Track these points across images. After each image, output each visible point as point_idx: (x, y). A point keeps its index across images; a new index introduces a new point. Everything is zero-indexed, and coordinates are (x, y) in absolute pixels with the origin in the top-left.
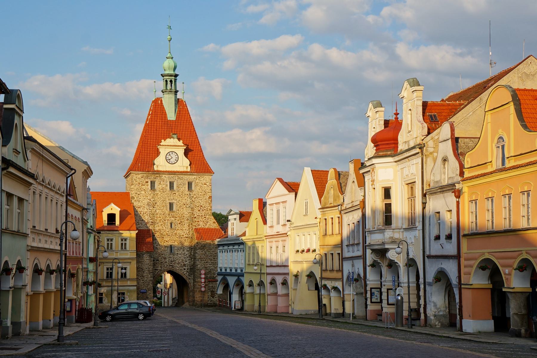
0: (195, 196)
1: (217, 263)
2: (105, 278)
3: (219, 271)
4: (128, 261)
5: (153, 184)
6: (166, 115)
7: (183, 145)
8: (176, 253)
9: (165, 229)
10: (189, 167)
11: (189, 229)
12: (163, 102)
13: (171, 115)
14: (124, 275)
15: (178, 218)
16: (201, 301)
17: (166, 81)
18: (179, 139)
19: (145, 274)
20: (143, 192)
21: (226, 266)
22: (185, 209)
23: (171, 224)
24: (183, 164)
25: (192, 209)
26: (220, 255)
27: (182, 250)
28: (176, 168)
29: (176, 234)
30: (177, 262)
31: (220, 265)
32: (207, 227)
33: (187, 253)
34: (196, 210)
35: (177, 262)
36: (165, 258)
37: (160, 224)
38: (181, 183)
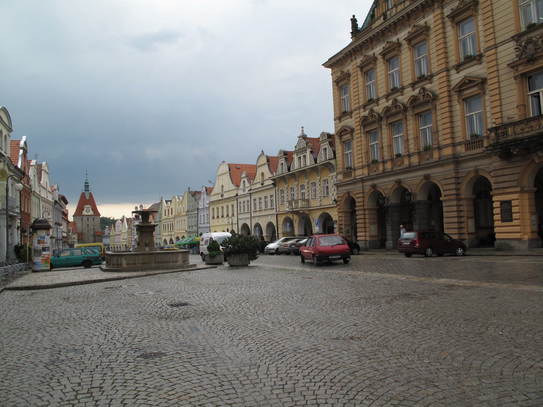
5: (82, 218)
13: (87, 198)
24: (91, 213)
28: (89, 214)
38: (91, 219)
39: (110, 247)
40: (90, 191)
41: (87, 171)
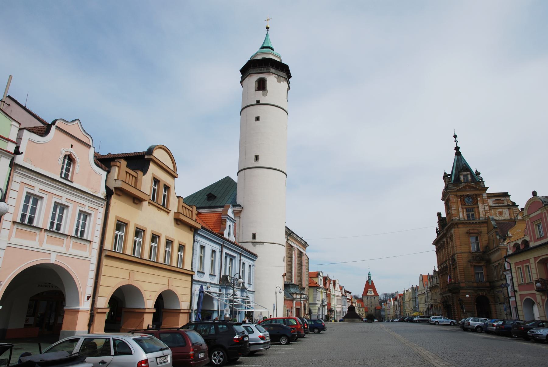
5: (367, 298)
24: (373, 294)
38: (373, 298)
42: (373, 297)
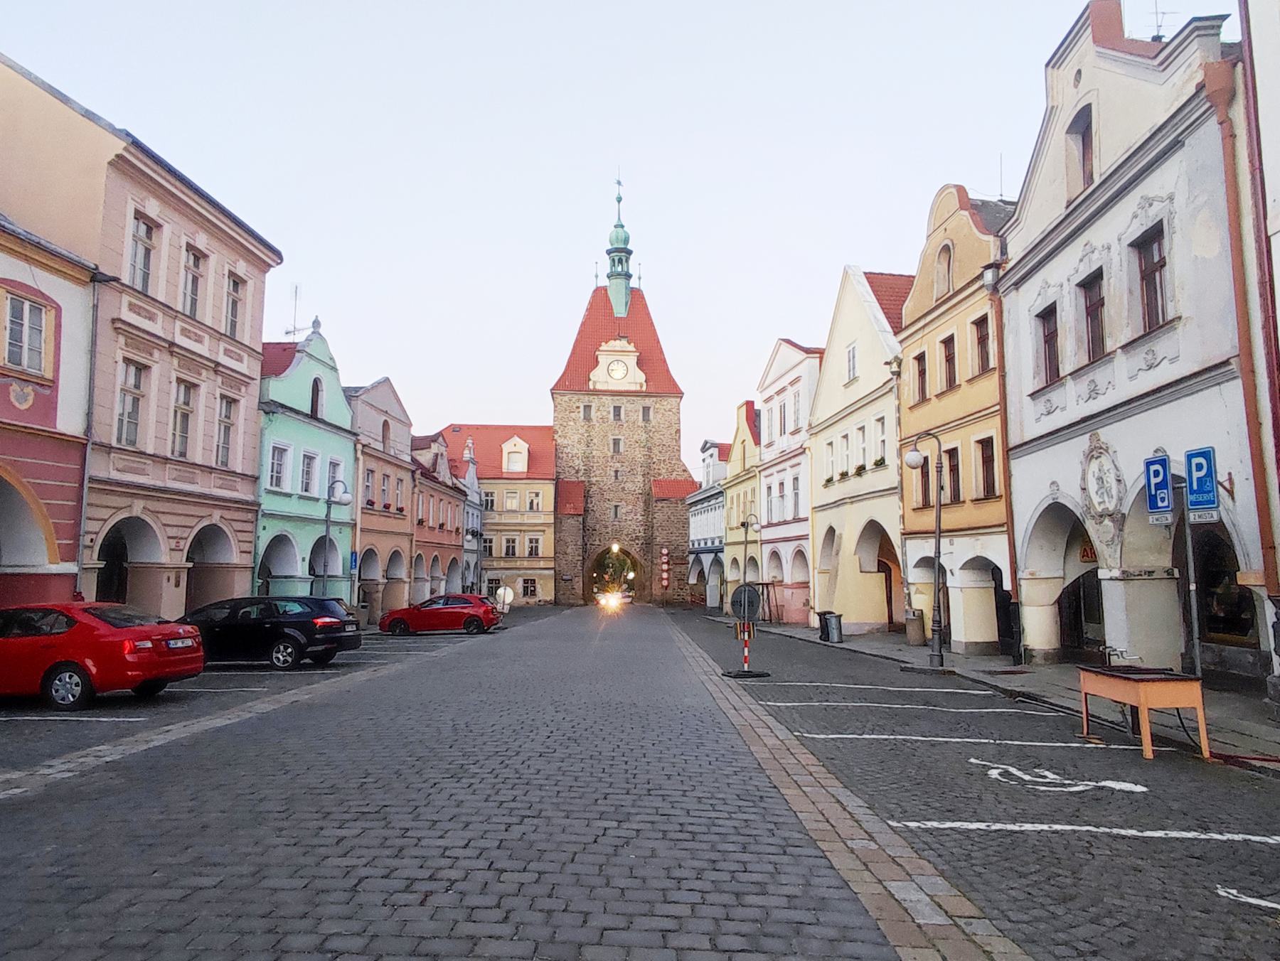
0: (653, 430)
1: (687, 535)
2: (503, 555)
3: (691, 547)
4: (541, 528)
5: (587, 408)
6: (612, 309)
7: (634, 350)
8: (624, 518)
9: (605, 480)
10: (645, 384)
11: (644, 481)
12: (609, 292)
14: (533, 553)
15: (627, 463)
16: (662, 594)
17: (613, 260)
18: (629, 343)
19: (569, 551)
20: (572, 423)
21: (699, 537)
22: (637, 449)
23: (616, 472)
24: (636, 379)
25: (650, 449)
26: (692, 520)
27: (633, 514)
29: (623, 489)
30: (625, 532)
31: (692, 538)
32: (673, 477)
33: (641, 518)
34: (655, 451)
35: (625, 532)
36: (606, 527)
37: (598, 472)
38: (632, 409)
39: (726, 558)
40: (634, 283)
41: (619, 183)
42: (641, 403)
